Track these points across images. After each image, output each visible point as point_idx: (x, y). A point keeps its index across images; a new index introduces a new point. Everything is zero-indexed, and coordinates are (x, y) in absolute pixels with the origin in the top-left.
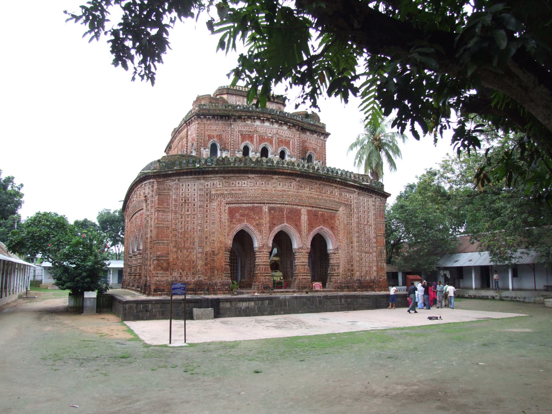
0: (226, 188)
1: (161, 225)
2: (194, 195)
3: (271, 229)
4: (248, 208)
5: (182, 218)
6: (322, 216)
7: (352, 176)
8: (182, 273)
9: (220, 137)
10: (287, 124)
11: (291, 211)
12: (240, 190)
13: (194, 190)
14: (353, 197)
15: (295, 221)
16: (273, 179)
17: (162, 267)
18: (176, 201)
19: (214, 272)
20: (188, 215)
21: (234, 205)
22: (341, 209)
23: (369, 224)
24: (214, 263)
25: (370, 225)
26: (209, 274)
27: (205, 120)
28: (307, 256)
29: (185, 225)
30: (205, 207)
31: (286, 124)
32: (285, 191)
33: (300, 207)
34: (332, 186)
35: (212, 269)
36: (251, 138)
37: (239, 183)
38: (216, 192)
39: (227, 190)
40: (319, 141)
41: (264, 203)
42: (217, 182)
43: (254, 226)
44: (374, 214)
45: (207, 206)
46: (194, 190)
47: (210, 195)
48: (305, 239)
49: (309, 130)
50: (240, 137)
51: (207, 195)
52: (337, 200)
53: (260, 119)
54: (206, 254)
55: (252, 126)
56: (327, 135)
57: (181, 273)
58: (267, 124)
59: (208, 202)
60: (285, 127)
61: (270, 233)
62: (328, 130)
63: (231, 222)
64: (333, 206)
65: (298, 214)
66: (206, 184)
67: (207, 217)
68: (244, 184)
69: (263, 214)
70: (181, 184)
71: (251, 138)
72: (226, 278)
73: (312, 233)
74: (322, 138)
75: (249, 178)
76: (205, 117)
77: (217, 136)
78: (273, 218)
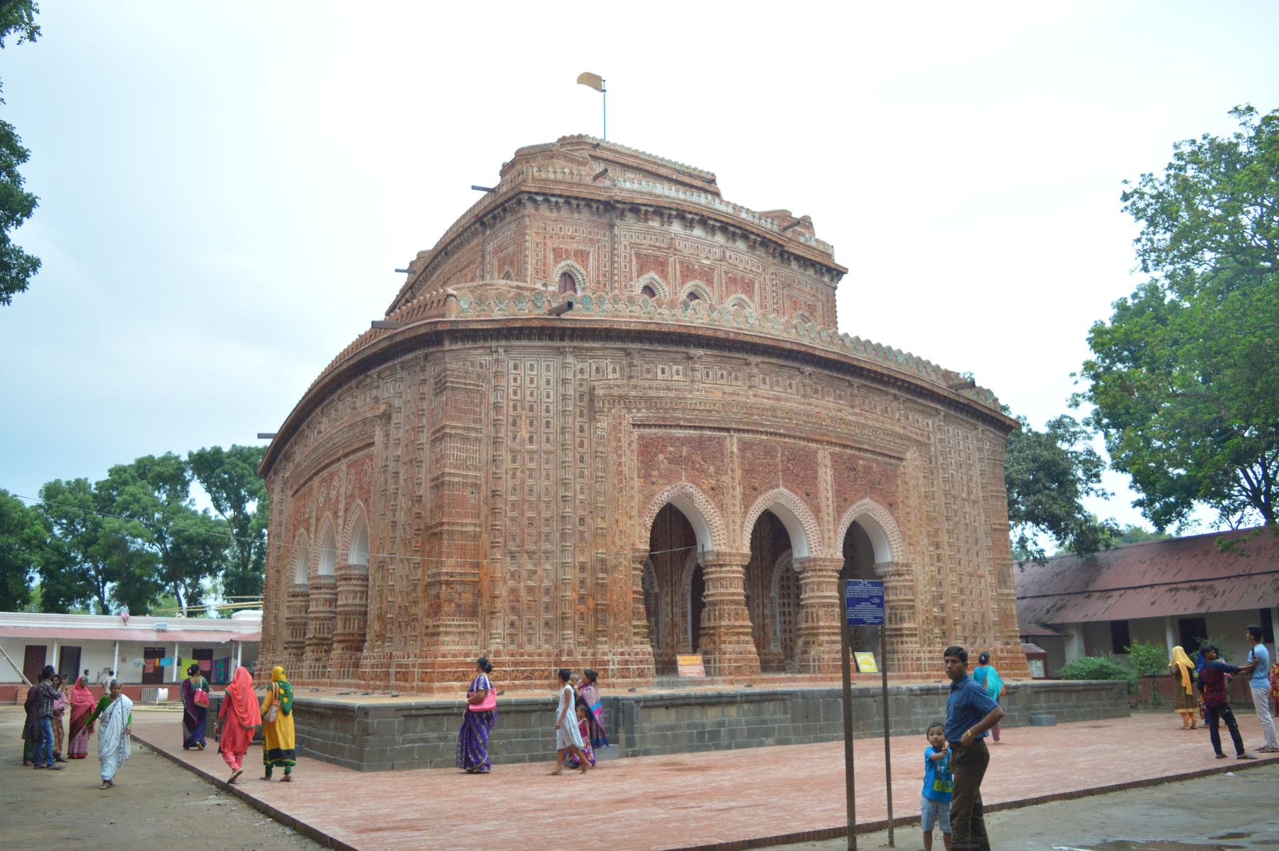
1: (457, 480)
2: (548, 396)
4: (689, 440)
5: (514, 461)
6: (867, 470)
8: (517, 623)
12: (669, 389)
13: (548, 382)
16: (748, 364)
17: (458, 606)
19: (604, 622)
21: (654, 430)
22: (908, 456)
23: (973, 497)
25: (975, 502)
26: (590, 628)
27: (544, 210)
32: (778, 399)
33: (814, 446)
34: (887, 393)
35: (601, 613)
38: (607, 392)
39: (635, 387)
40: (820, 286)
41: (728, 430)
42: (607, 364)
43: (703, 491)
44: (982, 474)
45: (582, 430)
47: (592, 400)
48: (832, 534)
52: (901, 431)
56: (838, 273)
58: (698, 232)
59: (585, 419)
60: (741, 245)
61: (746, 513)
62: (839, 260)
63: (647, 476)
64: (892, 446)
66: (579, 366)
70: (511, 364)
71: (661, 266)
72: (637, 639)
74: (826, 279)
75: (689, 358)
76: (547, 201)
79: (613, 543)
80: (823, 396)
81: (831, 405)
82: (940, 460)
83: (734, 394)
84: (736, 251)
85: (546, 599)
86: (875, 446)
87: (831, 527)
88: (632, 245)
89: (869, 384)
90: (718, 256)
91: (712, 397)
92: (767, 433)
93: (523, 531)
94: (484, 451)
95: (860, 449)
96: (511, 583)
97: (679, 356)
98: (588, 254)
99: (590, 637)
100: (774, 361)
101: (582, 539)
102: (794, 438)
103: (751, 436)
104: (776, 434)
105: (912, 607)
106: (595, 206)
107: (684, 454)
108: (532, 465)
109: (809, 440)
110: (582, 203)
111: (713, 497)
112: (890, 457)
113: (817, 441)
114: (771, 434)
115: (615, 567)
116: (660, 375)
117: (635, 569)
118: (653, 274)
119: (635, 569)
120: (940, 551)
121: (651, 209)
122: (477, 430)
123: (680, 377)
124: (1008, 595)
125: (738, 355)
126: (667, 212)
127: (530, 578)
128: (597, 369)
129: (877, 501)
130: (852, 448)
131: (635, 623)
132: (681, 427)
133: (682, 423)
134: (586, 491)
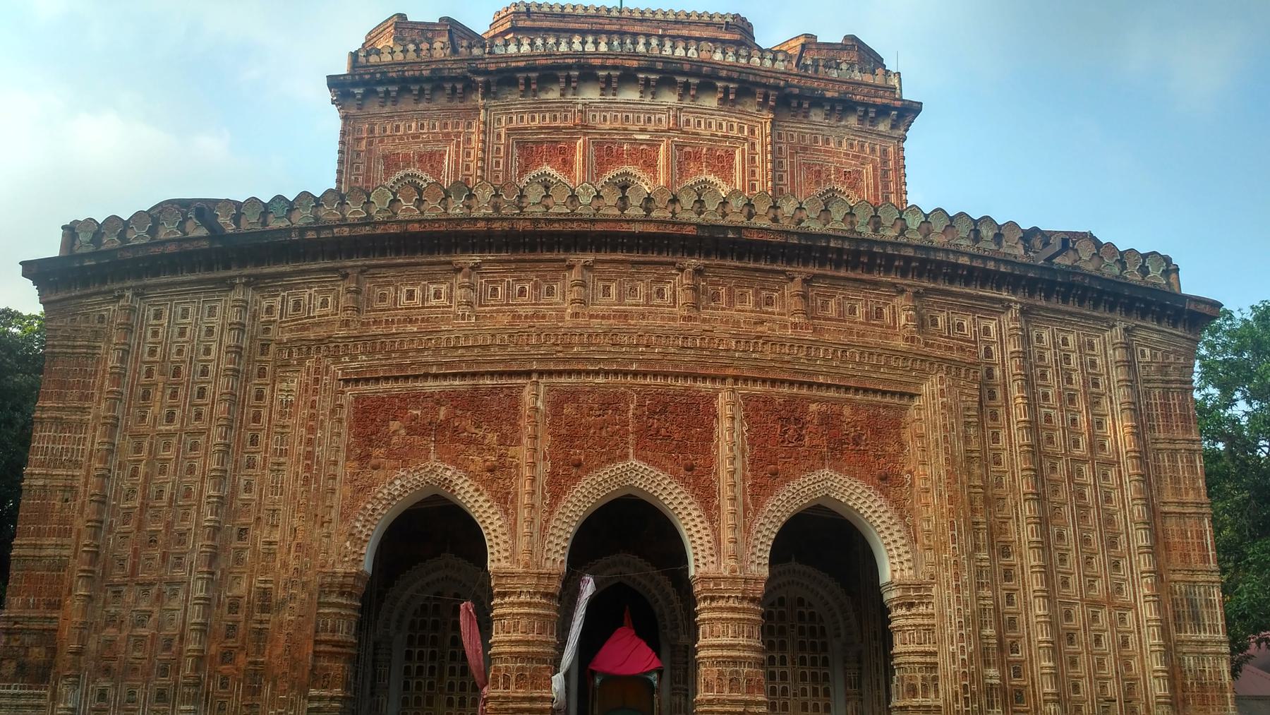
0: (343, 316)
2: (207, 351)
3: (557, 488)
7: (987, 233)
8: (111, 693)
10: (715, 89)
11: (661, 406)
13: (210, 331)
14: (1000, 332)
16: (571, 267)
18: (118, 377)
19: (257, 691)
20: (169, 434)
21: (383, 386)
22: (925, 388)
24: (259, 651)
25: (1110, 463)
28: (754, 614)
29: (148, 478)
30: (253, 402)
32: (625, 316)
34: (876, 284)
37: (411, 295)
38: (295, 335)
39: (346, 323)
41: (528, 374)
42: (311, 296)
43: (472, 476)
45: (260, 396)
46: (210, 331)
49: (818, 101)
50: (515, 151)
51: (265, 347)
53: (596, 79)
55: (565, 107)
56: (911, 110)
57: (102, 695)
60: (711, 102)
62: (909, 94)
63: (364, 458)
64: (884, 373)
65: (699, 415)
66: (265, 304)
67: (254, 441)
68: (437, 295)
69: (522, 423)
73: (770, 504)
74: (883, 127)
76: (370, 93)
77: (421, 156)
79: (285, 565)
80: (731, 303)
81: (741, 317)
82: (1015, 391)
83: (535, 315)
85: (165, 655)
89: (828, 271)
90: (664, 126)
91: (489, 324)
92: (607, 373)
93: (135, 551)
94: (89, 439)
95: (810, 385)
97: (437, 268)
98: (442, 156)
100: (619, 256)
102: (666, 376)
103: (573, 379)
104: (626, 374)
105: (934, 666)
108: (167, 455)
109: (695, 378)
110: (427, 87)
111: (487, 484)
112: (884, 393)
113: (714, 379)
114: (616, 373)
115: (284, 602)
117: (330, 605)
118: (548, 169)
119: (330, 605)
120: (1014, 559)
121: (534, 75)
122: (83, 410)
123: (443, 301)
124: (1203, 643)
125: (548, 256)
127: (141, 623)
128: (297, 306)
129: (851, 474)
130: (792, 383)
131: (313, 692)
132: (436, 376)
133: (434, 370)
134: (256, 489)
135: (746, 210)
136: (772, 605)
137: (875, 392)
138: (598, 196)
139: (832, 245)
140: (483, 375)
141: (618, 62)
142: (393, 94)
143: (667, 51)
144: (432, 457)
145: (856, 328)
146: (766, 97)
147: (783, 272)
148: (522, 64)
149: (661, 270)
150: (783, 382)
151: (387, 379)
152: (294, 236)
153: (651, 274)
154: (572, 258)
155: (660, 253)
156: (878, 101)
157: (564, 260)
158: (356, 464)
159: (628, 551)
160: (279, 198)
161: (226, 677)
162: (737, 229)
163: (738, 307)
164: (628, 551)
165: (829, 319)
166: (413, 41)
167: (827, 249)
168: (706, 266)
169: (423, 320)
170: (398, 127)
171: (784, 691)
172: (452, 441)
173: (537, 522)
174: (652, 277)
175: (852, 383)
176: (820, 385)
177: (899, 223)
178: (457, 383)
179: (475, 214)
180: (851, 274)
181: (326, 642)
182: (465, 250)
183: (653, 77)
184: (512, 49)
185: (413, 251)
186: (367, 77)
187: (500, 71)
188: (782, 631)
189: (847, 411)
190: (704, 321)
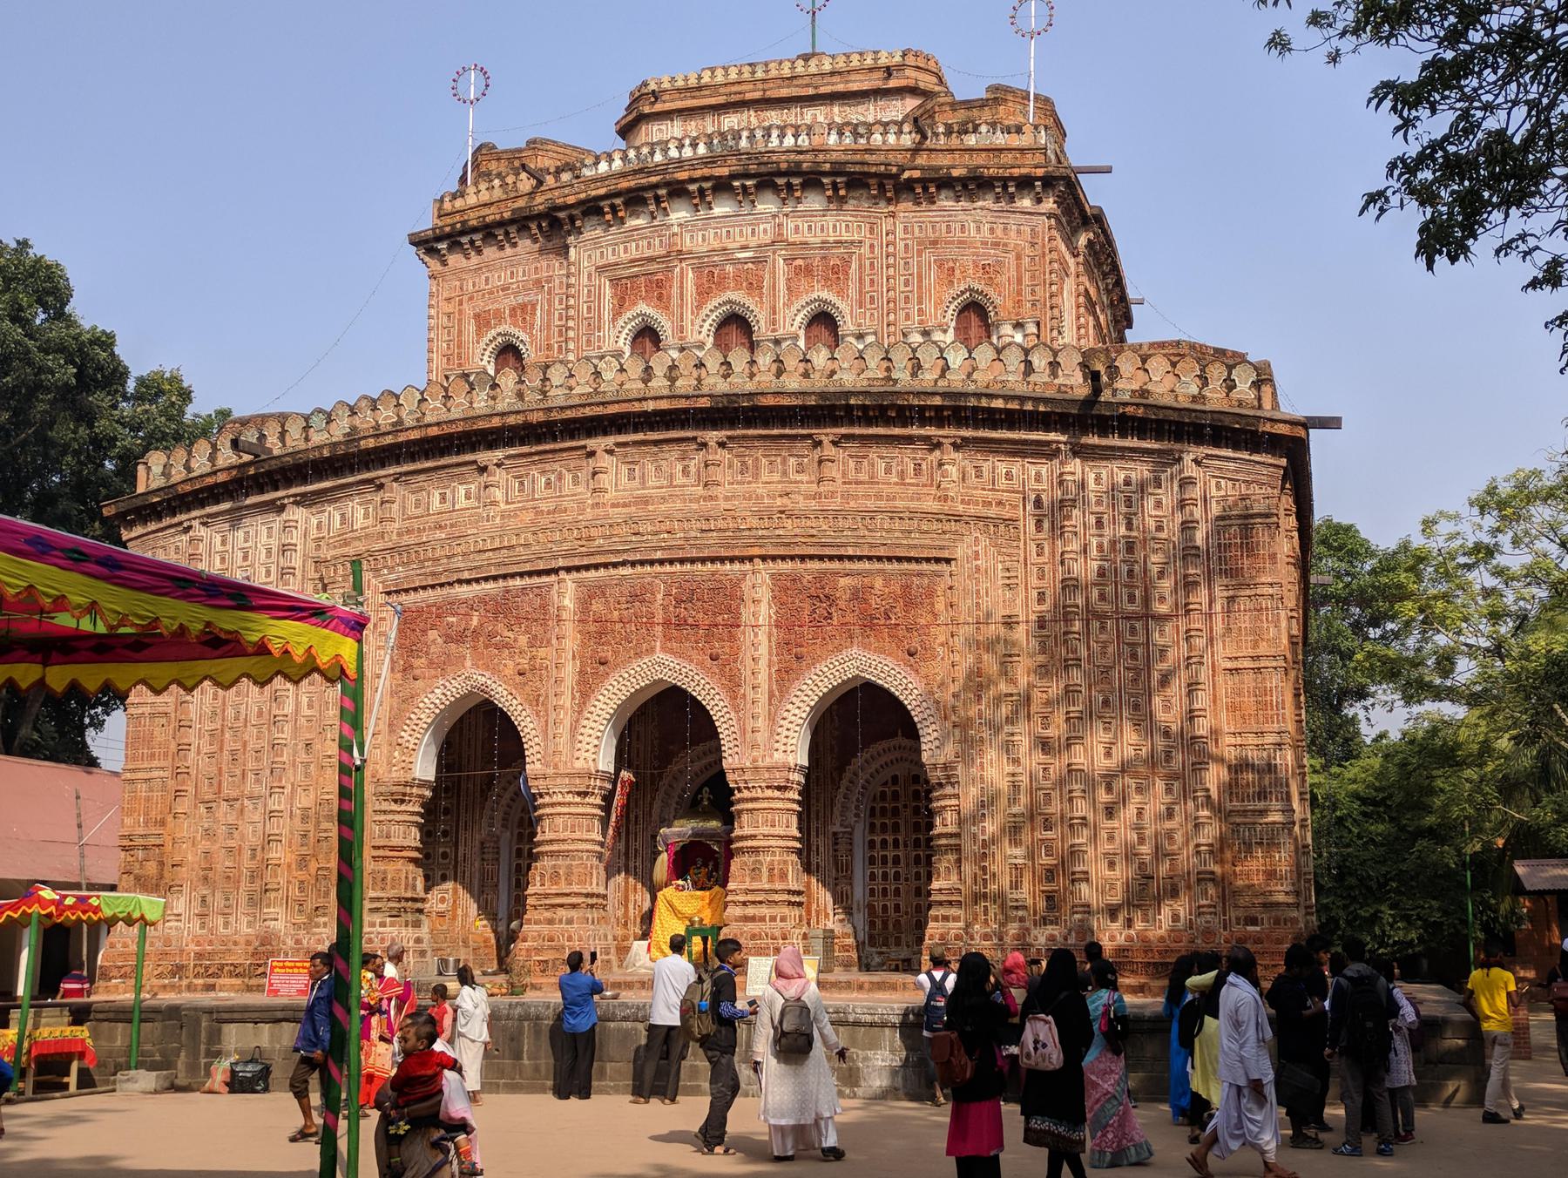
4: (483, 601)
8: (209, 899)
9: (522, 312)
13: (269, 552)
15: (708, 637)
16: (592, 454)
17: (138, 878)
26: (309, 906)
27: (455, 260)
31: (812, 180)
32: (645, 501)
36: (658, 290)
40: (1013, 220)
41: (556, 571)
43: (506, 680)
49: (946, 183)
50: (608, 291)
54: (305, 819)
65: (728, 601)
68: (468, 497)
70: (218, 539)
71: (658, 290)
74: (1026, 203)
75: (483, 470)
76: (455, 246)
77: (513, 310)
78: (600, 634)
80: (756, 476)
81: (761, 490)
84: (810, 214)
85: (253, 864)
86: (872, 545)
87: (762, 708)
88: (601, 269)
92: (633, 564)
95: (841, 558)
96: (204, 845)
98: (534, 307)
99: (310, 918)
100: (640, 436)
101: (307, 775)
102: (693, 561)
104: (652, 562)
106: (533, 226)
107: (475, 622)
109: (722, 560)
110: (512, 229)
113: (742, 560)
114: (642, 563)
116: (436, 503)
118: (642, 307)
121: (618, 201)
126: (649, 195)
129: (881, 651)
130: (821, 558)
132: (468, 582)
133: (466, 575)
134: (316, 705)
135: (774, 366)
136: (885, 784)
137: (909, 559)
138: (622, 370)
139: (852, 402)
140: (513, 576)
141: (706, 172)
142: (478, 243)
143: (774, 142)
144: (468, 663)
145: (887, 490)
146: (881, 187)
147: (810, 436)
148: (602, 191)
149: (683, 446)
150: (812, 557)
151: (424, 588)
152: (326, 453)
153: (673, 453)
154: (591, 443)
155: (683, 428)
156: (1016, 172)
157: (585, 447)
158: (399, 675)
159: (668, 743)
160: (320, 411)
161: (302, 882)
162: (751, 395)
163: (764, 479)
164: (668, 743)
165: (861, 483)
166: (499, 175)
167: (849, 408)
168: (729, 438)
169: (452, 526)
170: (487, 279)
171: (897, 876)
172: (486, 647)
173: (567, 722)
174: (676, 454)
175: (882, 552)
176: (850, 558)
177: (941, 362)
178: (490, 585)
179: (500, 407)
180: (881, 431)
181: (383, 847)
182: (491, 446)
183: (749, 183)
184: (603, 167)
185: (443, 453)
186: (448, 229)
187: (581, 203)
188: (895, 812)
189: (879, 583)
190: (727, 499)
